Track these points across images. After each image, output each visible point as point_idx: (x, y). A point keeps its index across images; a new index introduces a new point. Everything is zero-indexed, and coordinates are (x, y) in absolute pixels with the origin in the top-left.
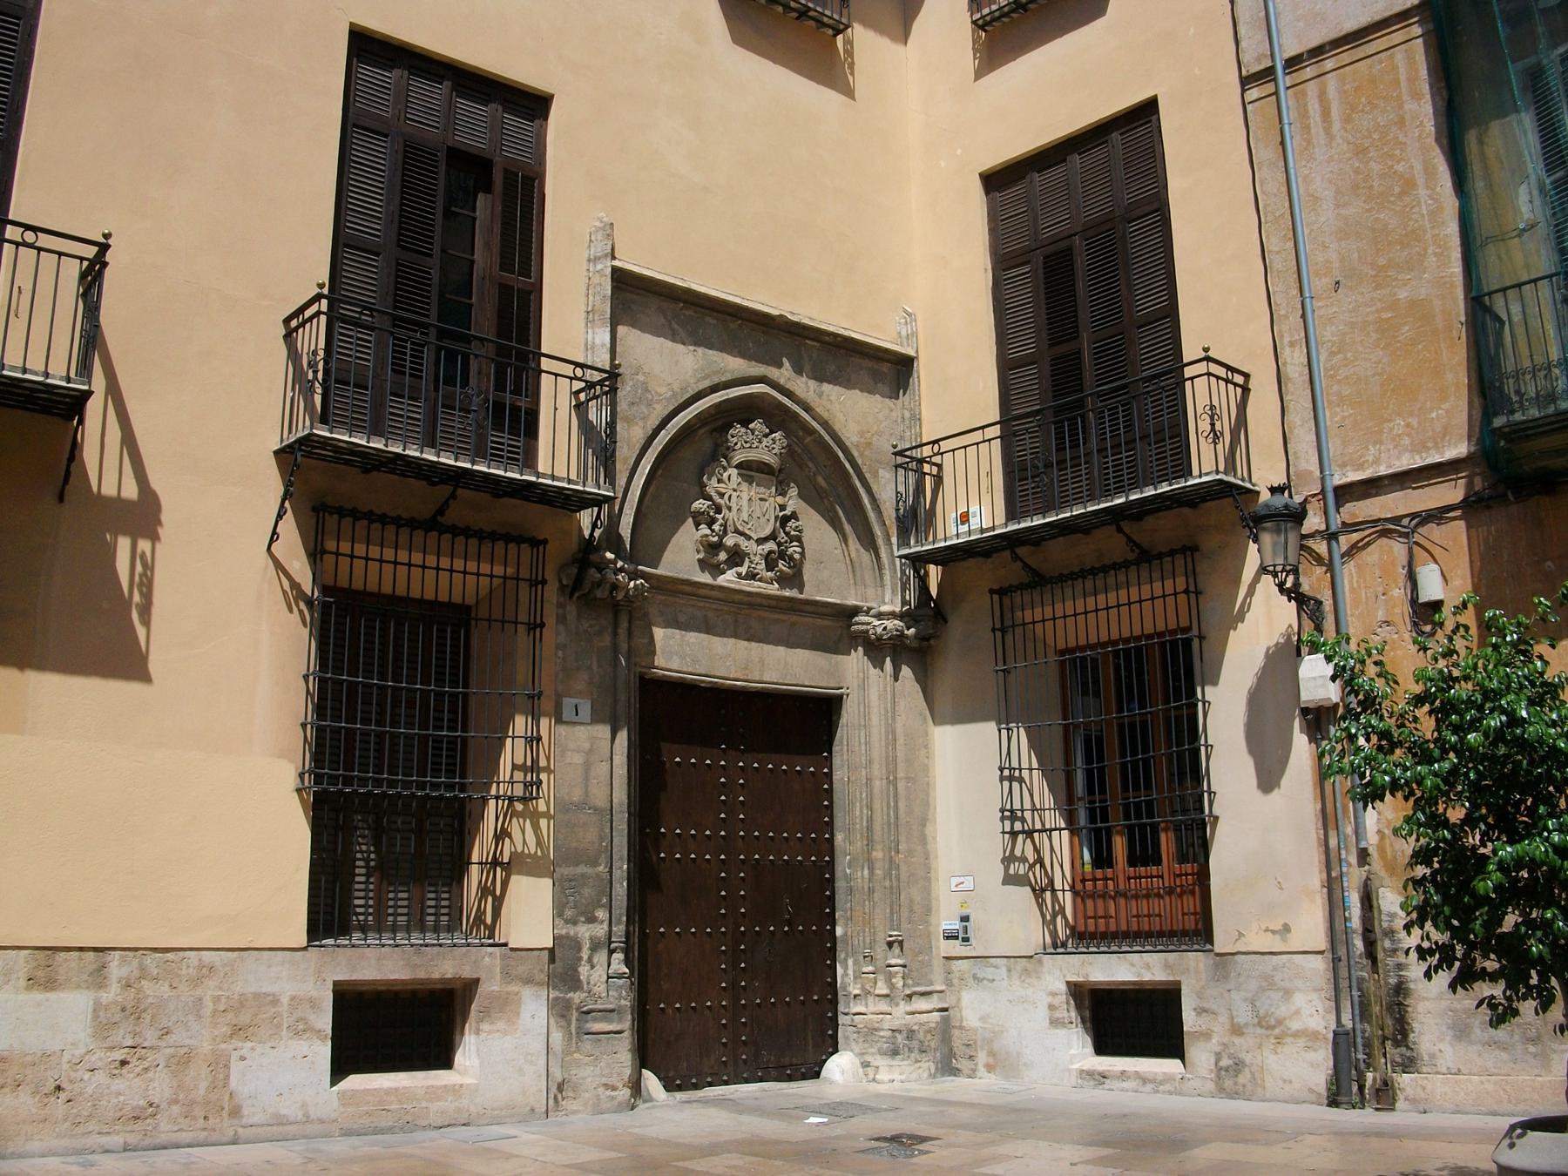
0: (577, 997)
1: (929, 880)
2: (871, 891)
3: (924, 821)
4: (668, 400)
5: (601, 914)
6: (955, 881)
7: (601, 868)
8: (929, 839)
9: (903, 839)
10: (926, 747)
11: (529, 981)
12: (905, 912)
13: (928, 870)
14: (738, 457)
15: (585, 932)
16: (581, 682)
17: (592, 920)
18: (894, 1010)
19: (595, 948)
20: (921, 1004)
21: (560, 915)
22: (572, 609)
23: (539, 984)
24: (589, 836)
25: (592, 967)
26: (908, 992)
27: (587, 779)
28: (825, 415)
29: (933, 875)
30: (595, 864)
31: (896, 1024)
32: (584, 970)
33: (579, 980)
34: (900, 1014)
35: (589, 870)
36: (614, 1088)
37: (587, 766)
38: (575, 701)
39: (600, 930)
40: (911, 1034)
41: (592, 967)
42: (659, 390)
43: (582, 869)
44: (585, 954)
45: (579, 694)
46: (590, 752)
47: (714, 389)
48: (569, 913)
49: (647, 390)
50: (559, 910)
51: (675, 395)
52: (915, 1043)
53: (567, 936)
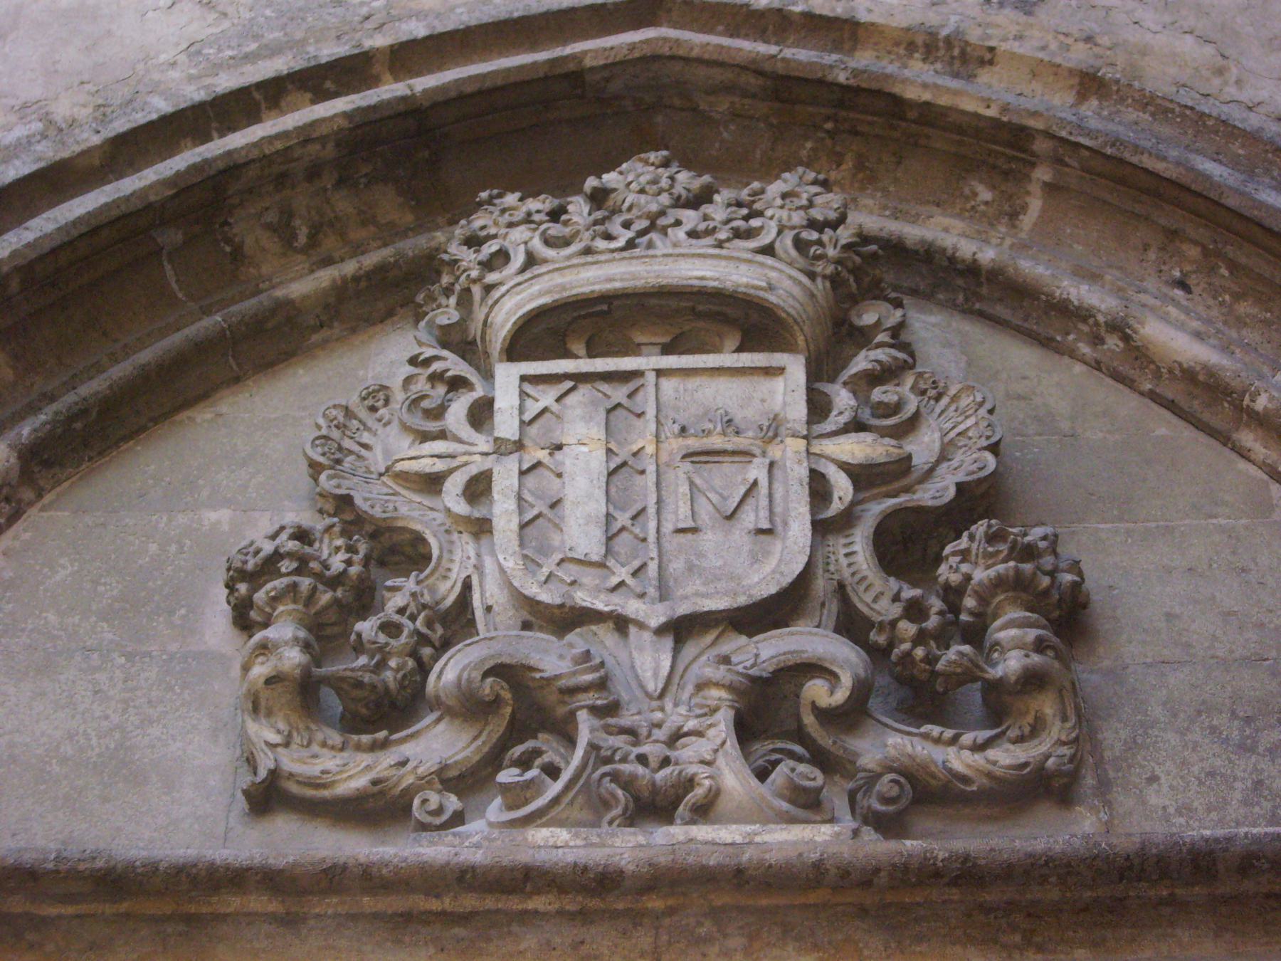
14: (509, 308)
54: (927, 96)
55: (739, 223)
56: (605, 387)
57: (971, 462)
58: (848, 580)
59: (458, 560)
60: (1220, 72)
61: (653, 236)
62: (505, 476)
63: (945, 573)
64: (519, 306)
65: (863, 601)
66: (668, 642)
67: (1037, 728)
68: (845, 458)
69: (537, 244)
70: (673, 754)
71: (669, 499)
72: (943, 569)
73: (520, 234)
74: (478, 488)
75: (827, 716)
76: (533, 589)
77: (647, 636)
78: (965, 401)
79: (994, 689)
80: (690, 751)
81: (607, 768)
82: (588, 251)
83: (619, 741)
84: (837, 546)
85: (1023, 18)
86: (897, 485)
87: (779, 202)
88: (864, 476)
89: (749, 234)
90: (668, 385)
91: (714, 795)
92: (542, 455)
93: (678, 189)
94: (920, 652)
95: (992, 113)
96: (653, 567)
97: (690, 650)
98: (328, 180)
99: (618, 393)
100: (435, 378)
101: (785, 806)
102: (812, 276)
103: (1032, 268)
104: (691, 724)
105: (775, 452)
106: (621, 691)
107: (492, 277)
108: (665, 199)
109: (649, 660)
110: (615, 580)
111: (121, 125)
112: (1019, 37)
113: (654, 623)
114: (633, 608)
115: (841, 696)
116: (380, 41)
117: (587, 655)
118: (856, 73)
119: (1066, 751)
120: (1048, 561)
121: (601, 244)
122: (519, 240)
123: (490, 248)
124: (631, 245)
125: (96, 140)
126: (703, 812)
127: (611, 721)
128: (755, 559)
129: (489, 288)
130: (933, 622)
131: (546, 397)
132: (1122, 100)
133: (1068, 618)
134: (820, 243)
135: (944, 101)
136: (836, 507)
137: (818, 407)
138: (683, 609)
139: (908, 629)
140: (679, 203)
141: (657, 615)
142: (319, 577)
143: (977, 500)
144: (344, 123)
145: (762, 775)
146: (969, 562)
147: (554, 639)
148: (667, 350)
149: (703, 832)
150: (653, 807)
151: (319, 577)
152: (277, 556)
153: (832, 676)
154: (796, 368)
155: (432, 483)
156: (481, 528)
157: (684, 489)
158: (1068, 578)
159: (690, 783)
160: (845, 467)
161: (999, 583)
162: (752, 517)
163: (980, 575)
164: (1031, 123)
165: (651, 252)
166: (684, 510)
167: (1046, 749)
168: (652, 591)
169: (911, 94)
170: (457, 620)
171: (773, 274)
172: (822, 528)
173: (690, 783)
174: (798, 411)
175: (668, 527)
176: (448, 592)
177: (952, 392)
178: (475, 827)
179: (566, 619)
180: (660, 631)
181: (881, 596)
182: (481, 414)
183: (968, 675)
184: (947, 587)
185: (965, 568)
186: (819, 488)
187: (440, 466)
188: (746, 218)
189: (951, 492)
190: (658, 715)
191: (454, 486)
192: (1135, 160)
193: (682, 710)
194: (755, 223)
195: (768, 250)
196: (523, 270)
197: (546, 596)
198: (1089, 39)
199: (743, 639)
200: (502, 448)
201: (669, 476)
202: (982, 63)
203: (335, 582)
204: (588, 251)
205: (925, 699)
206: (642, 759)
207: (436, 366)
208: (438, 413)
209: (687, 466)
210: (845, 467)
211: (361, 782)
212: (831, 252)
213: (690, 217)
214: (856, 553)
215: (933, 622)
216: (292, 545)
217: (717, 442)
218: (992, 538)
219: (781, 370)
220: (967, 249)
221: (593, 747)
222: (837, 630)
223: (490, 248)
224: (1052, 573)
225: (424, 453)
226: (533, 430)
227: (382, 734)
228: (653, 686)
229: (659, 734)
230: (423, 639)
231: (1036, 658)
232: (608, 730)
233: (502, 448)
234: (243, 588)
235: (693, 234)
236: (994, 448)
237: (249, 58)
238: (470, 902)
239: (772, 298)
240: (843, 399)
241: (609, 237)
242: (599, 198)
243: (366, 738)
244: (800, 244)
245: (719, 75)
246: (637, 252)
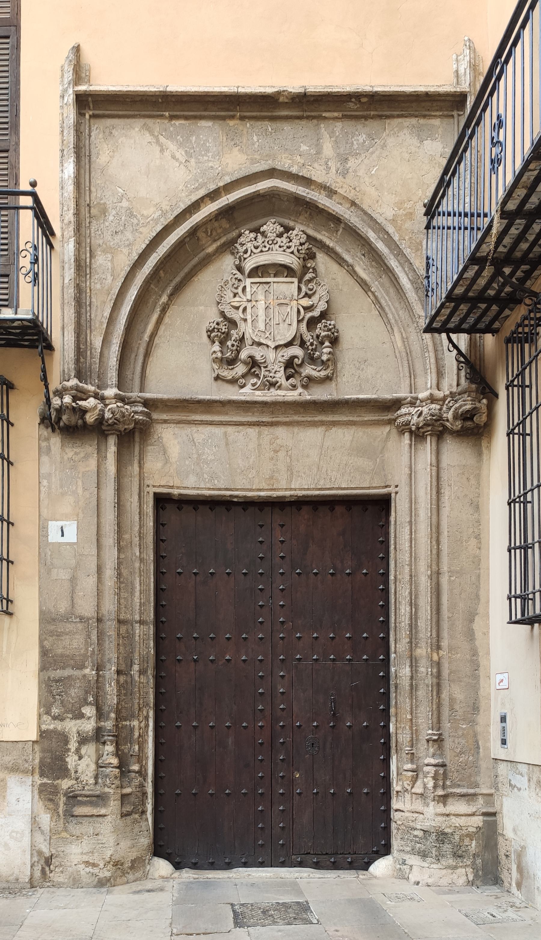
0: (65, 784)
1: (476, 678)
2: (413, 688)
3: (471, 617)
4: (156, 221)
5: (89, 711)
6: (499, 677)
7: (87, 671)
8: (478, 635)
9: (445, 634)
10: (478, 537)
11: (14, 769)
12: (446, 712)
13: (476, 666)
15: (72, 727)
16: (67, 505)
17: (81, 716)
18: (425, 810)
19: (83, 740)
20: (461, 807)
21: (48, 713)
22: (56, 441)
23: (25, 772)
24: (75, 643)
25: (80, 758)
26: (440, 792)
27: (73, 592)
28: (351, 196)
29: (482, 673)
30: (82, 667)
31: (427, 825)
32: (71, 760)
33: (67, 770)
34: (430, 815)
35: (77, 673)
36: (94, 865)
37: (73, 580)
38: (60, 523)
39: (89, 726)
40: (442, 836)
41: (80, 758)
42: (145, 213)
43: (68, 672)
44: (73, 745)
45: (66, 517)
46: (76, 568)
47: (213, 195)
48: (55, 711)
49: (131, 215)
50: (45, 706)
51: (164, 214)
52: (447, 848)
53: (55, 731)
54: (323, 207)
55: (287, 244)
56: (264, 285)
57: (322, 306)
58: (303, 333)
59: (242, 326)
60: (377, 202)
61: (273, 245)
62: (249, 310)
63: (318, 331)
64: (250, 266)
65: (304, 337)
66: (275, 350)
67: (328, 367)
68: (303, 305)
69: (252, 248)
70: (275, 375)
71: (275, 318)
72: (317, 331)
73: (249, 245)
74: (245, 309)
75: (297, 365)
76: (254, 338)
77: (272, 350)
78: (324, 287)
79: (322, 361)
80: (278, 375)
81: (266, 379)
82: (262, 251)
83: (267, 373)
84: (301, 324)
85: (343, 180)
86: (311, 309)
87: (295, 238)
88: (305, 308)
89: (289, 247)
90: (275, 284)
91: (281, 384)
92: (254, 303)
93: (277, 232)
94: (312, 352)
95: (334, 213)
96: (272, 333)
97: (278, 351)
98: (214, 220)
99: (267, 286)
100: (236, 279)
101: (290, 387)
102: (299, 258)
103: (339, 249)
104: (278, 370)
105: (292, 303)
106: (268, 362)
107: (245, 256)
108: (275, 234)
109: (271, 355)
110: (266, 336)
111: (176, 213)
112: (342, 187)
113: (273, 347)
114: (269, 343)
115: (300, 362)
116: (221, 184)
117: (262, 356)
118: (311, 199)
119: (332, 371)
120: (333, 330)
121: (264, 249)
122: (250, 246)
123: (244, 248)
124: (269, 248)
125: (172, 218)
126: (280, 388)
127: (266, 369)
128: (289, 330)
129: (245, 259)
130: (314, 347)
131: (255, 287)
132: (359, 208)
133: (335, 341)
134: (302, 250)
135: (326, 209)
136: (301, 317)
137: (300, 289)
138: (277, 344)
139: (310, 347)
140: (277, 236)
141: (272, 345)
142: (221, 333)
143: (324, 315)
144: (216, 212)
145: (288, 379)
146: (320, 330)
147: (257, 348)
148: (275, 276)
149: (279, 392)
150: (273, 385)
151: (221, 333)
152: (214, 328)
153: (299, 359)
154: (296, 280)
155: (237, 308)
156: (245, 320)
157: (277, 313)
158: (336, 334)
159: (277, 382)
160: (303, 307)
161: (325, 336)
162: (288, 321)
163: (323, 334)
164: (341, 218)
165: (272, 252)
166: (277, 319)
167: (328, 372)
168: (272, 339)
169: (320, 206)
170: (242, 340)
171: (293, 259)
172: (299, 321)
173: (277, 382)
174: (296, 293)
175: (275, 323)
176: (241, 334)
177: (322, 285)
178: (248, 389)
179: (260, 344)
180: (273, 349)
181: (308, 337)
182: (244, 288)
183: (319, 357)
184: (317, 335)
185: (320, 331)
186: (299, 311)
187: (238, 305)
188: (289, 242)
189: (319, 313)
190: (273, 367)
191: (241, 309)
192: (358, 231)
193: (276, 366)
194: (291, 244)
195: (292, 253)
196: (250, 255)
197: (257, 340)
198: (355, 189)
199: (286, 349)
200: (249, 301)
201: (275, 309)
202: (334, 193)
203: (223, 333)
204: (262, 251)
205: (312, 359)
206: (271, 377)
207: (236, 276)
208: (236, 288)
209: (278, 307)
210: (303, 307)
211: (231, 377)
212: (303, 252)
213: (278, 239)
214: (304, 325)
215: (314, 347)
216: (216, 326)
217: (282, 301)
218: (325, 326)
219: (293, 282)
220: (328, 242)
221: (264, 375)
222: (299, 346)
223: (244, 248)
224: (333, 333)
225: (235, 300)
226: (253, 296)
227: (232, 367)
228: (272, 361)
229: (273, 371)
230: (238, 346)
231: (329, 356)
232: (266, 371)
233: (249, 301)
234: (209, 333)
235: (280, 247)
236: (327, 302)
237: (197, 189)
238: (248, 405)
239: (292, 266)
240: (304, 289)
241: (265, 247)
242: (263, 234)
243: (230, 367)
244: (298, 251)
245: (285, 194)
246: (270, 252)
